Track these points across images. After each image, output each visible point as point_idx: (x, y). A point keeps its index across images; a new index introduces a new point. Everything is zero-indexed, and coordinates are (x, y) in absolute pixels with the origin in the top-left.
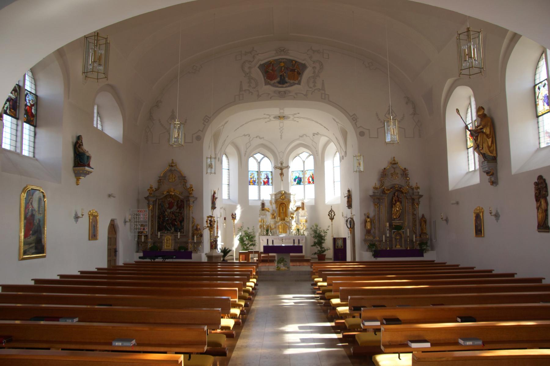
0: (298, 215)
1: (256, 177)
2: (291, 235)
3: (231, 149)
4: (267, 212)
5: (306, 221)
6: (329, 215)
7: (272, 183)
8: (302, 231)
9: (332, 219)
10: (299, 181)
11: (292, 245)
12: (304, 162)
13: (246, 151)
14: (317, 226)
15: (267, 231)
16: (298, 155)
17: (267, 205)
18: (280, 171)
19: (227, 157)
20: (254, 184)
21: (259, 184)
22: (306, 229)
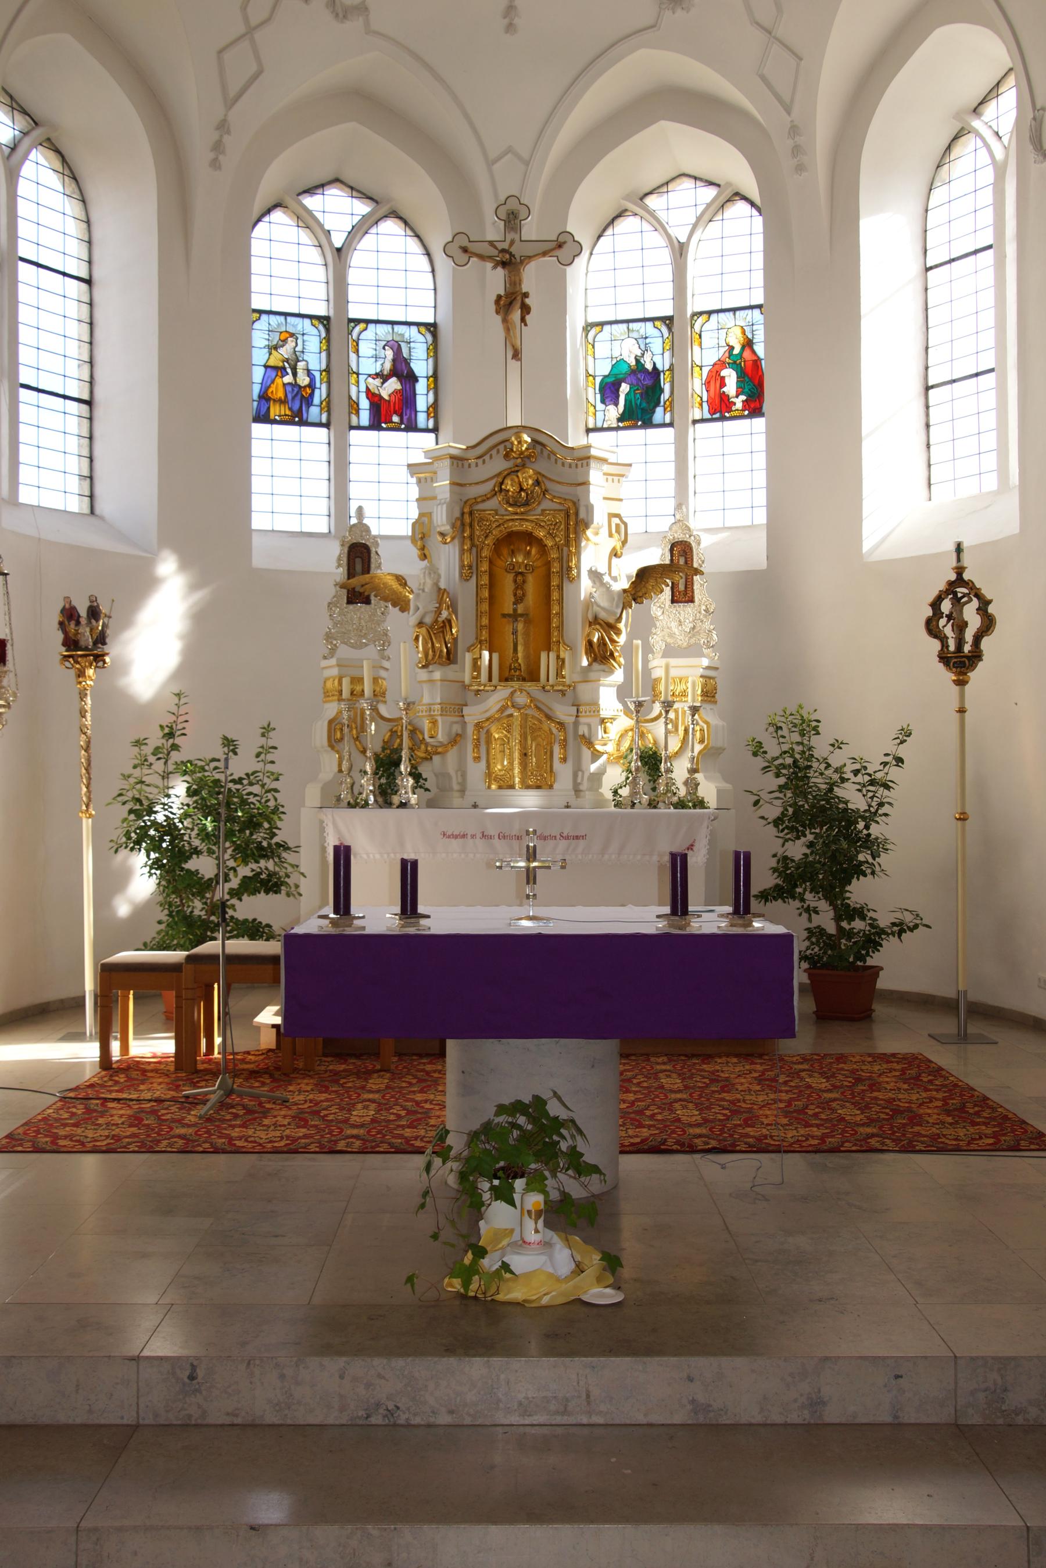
0: (644, 628)
1: (314, 358)
2: (585, 806)
3: (93, 98)
4: (394, 611)
5: (709, 694)
6: (932, 628)
7: (434, 410)
8: (680, 771)
9: (961, 662)
10: (641, 395)
11: (645, 917)
12: (680, 251)
13: (223, 126)
14: (808, 727)
15: (387, 764)
16: (634, 202)
17: (393, 563)
18: (496, 280)
19: (69, 171)
20: (298, 419)
21: (338, 421)
22: (711, 753)
